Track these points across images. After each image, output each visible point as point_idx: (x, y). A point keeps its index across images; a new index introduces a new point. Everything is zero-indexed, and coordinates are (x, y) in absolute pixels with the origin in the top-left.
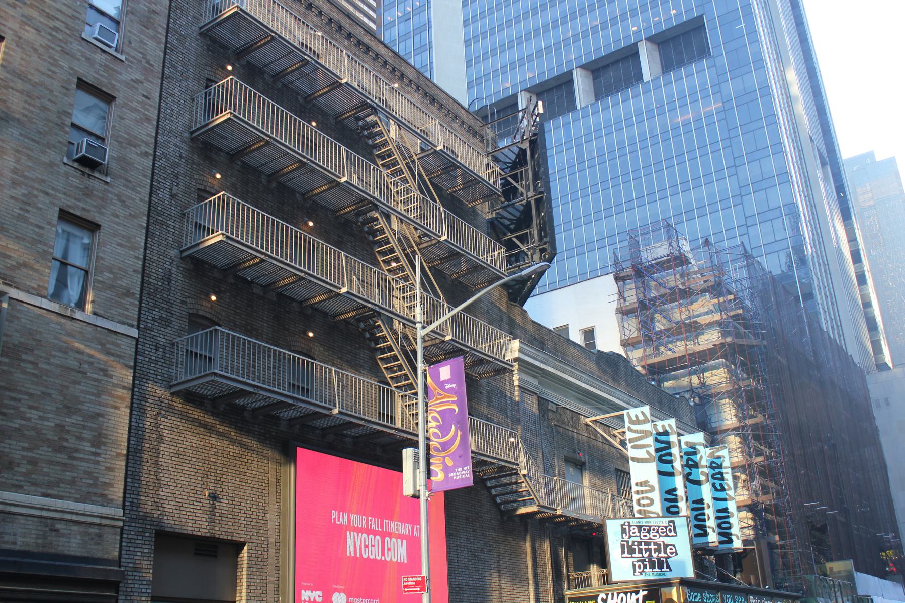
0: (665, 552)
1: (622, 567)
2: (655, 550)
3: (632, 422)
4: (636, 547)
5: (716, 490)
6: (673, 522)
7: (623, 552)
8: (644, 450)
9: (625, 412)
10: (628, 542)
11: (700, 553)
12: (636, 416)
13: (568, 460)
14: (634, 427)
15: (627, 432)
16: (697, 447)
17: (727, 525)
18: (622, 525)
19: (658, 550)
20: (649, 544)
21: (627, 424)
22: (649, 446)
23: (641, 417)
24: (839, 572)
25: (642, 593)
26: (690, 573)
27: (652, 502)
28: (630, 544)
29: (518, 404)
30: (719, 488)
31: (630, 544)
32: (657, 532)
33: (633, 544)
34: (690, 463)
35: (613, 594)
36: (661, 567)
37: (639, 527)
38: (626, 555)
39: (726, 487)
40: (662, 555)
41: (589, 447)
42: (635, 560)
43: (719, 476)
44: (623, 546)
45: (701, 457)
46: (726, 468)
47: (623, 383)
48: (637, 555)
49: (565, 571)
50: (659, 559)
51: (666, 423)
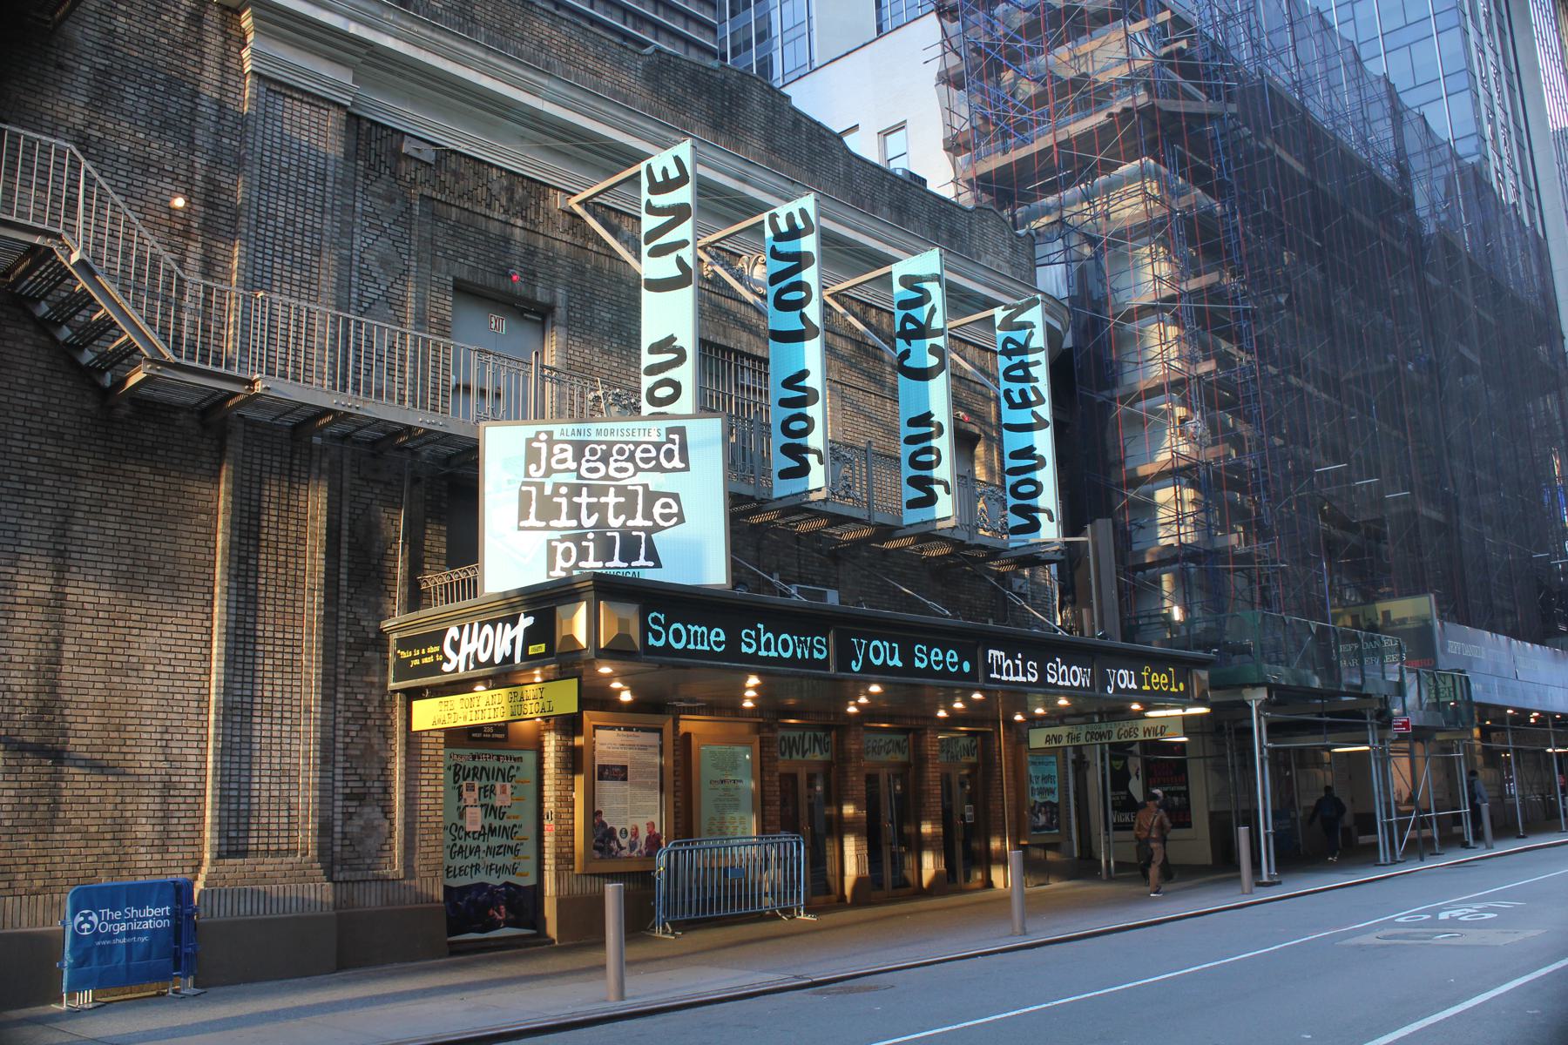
0: (648, 515)
1: (513, 554)
2: (619, 510)
3: (656, 188)
4: (564, 501)
5: (1013, 406)
6: (681, 431)
7: (524, 515)
8: (672, 257)
9: (643, 166)
10: (540, 487)
11: (746, 517)
12: (665, 172)
13: (464, 291)
14: (660, 200)
15: (645, 217)
16: (926, 285)
17: (1032, 488)
18: (529, 441)
19: (627, 509)
20: (603, 491)
21: (645, 195)
22: (684, 243)
23: (674, 173)
24: (1403, 621)
25: (525, 622)
26: (714, 571)
27: (1039, 487)
28: (548, 491)
29: (242, 120)
30: (1018, 400)
31: (548, 491)
32: (631, 458)
33: (556, 492)
34: (910, 326)
35: (471, 626)
36: (629, 554)
37: (579, 448)
38: (532, 521)
39: (1033, 398)
40: (639, 521)
41: (579, 271)
42: (557, 535)
43: (1020, 373)
44: (524, 499)
45: (933, 310)
46: (1036, 350)
47: (757, 144)
48: (564, 521)
49: (400, 570)
50: (626, 534)
51: (794, 207)
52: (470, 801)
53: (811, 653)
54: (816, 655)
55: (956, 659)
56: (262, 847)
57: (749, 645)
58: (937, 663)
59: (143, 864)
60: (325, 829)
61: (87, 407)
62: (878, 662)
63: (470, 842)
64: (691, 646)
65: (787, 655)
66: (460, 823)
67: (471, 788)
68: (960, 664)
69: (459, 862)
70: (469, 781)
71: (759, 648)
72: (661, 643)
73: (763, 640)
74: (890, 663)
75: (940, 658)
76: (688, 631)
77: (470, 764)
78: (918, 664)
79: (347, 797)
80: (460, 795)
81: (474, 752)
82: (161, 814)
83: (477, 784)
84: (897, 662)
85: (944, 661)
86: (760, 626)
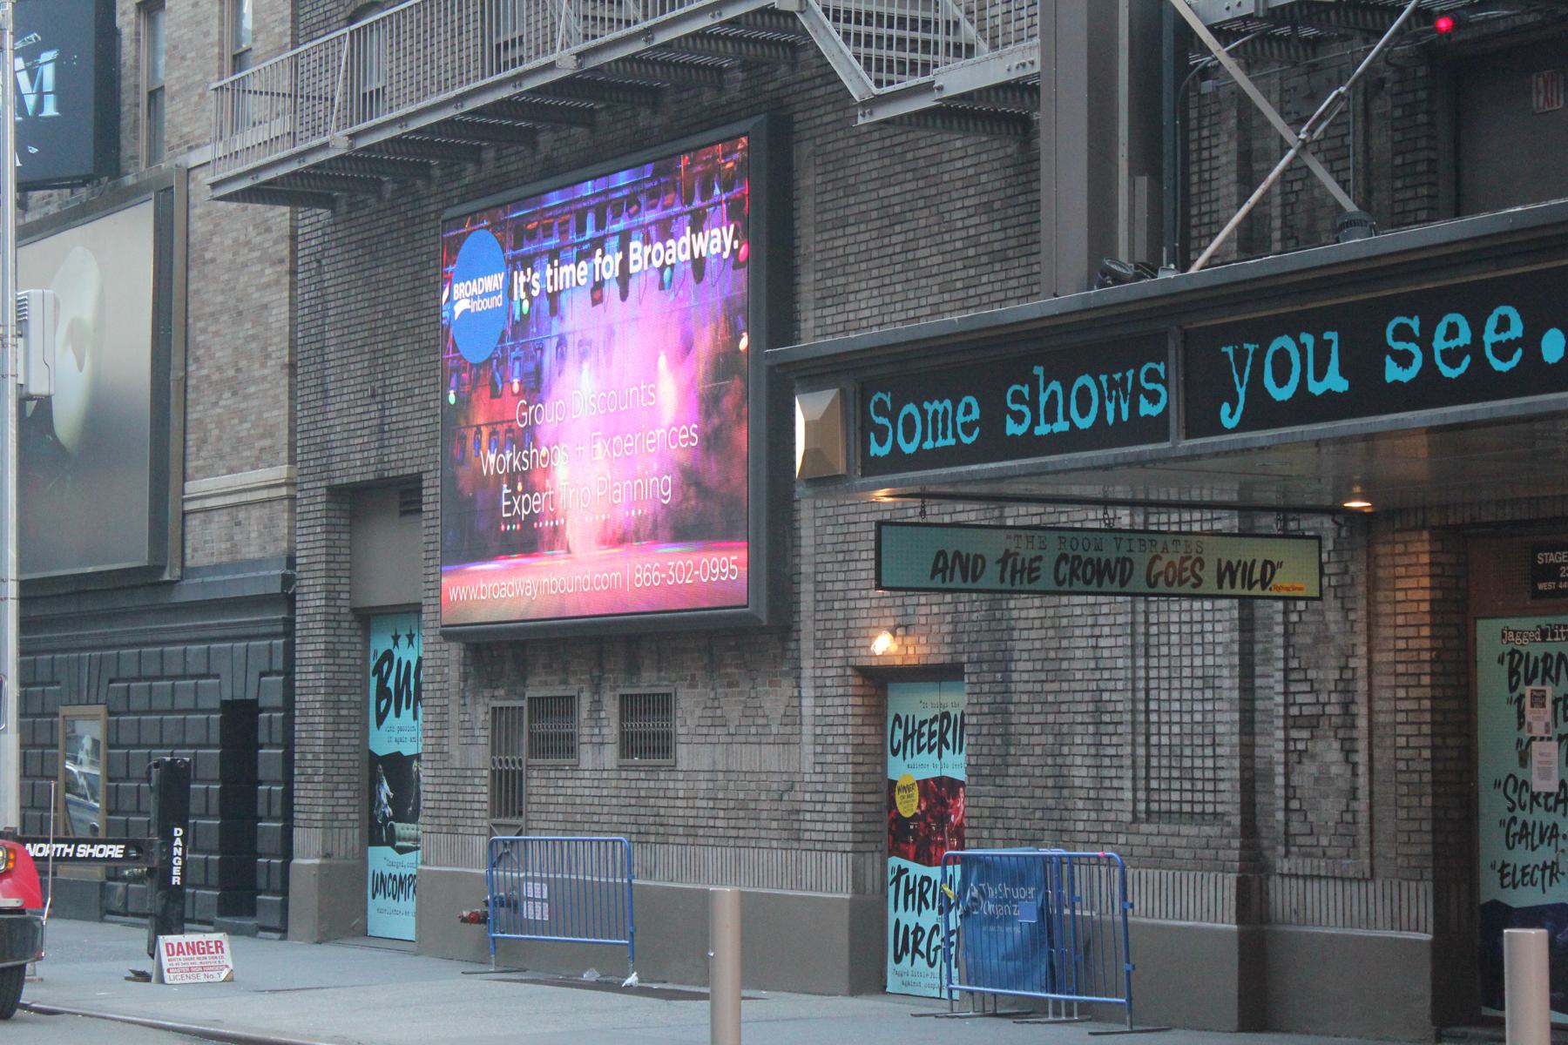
52: (1538, 730)
53: (1134, 408)
54: (1146, 408)
55: (1516, 330)
56: (1187, 808)
57: (1018, 417)
58: (1452, 357)
59: (1080, 826)
60: (1251, 781)
61: (1009, 151)
62: (1283, 394)
63: (1540, 816)
64: (928, 445)
65: (1085, 423)
66: (1521, 775)
67: (1538, 700)
68: (1531, 342)
69: (1521, 856)
70: (1536, 685)
71: (1035, 422)
72: (884, 451)
73: (1043, 398)
74: (1316, 388)
75: (1465, 337)
76: (924, 413)
77: (1537, 650)
78: (1393, 373)
79: (1291, 723)
80: (1521, 715)
81: (1544, 621)
82: (1093, 751)
83: (1550, 691)
84: (1336, 382)
85: (1476, 346)
86: (1039, 371)
